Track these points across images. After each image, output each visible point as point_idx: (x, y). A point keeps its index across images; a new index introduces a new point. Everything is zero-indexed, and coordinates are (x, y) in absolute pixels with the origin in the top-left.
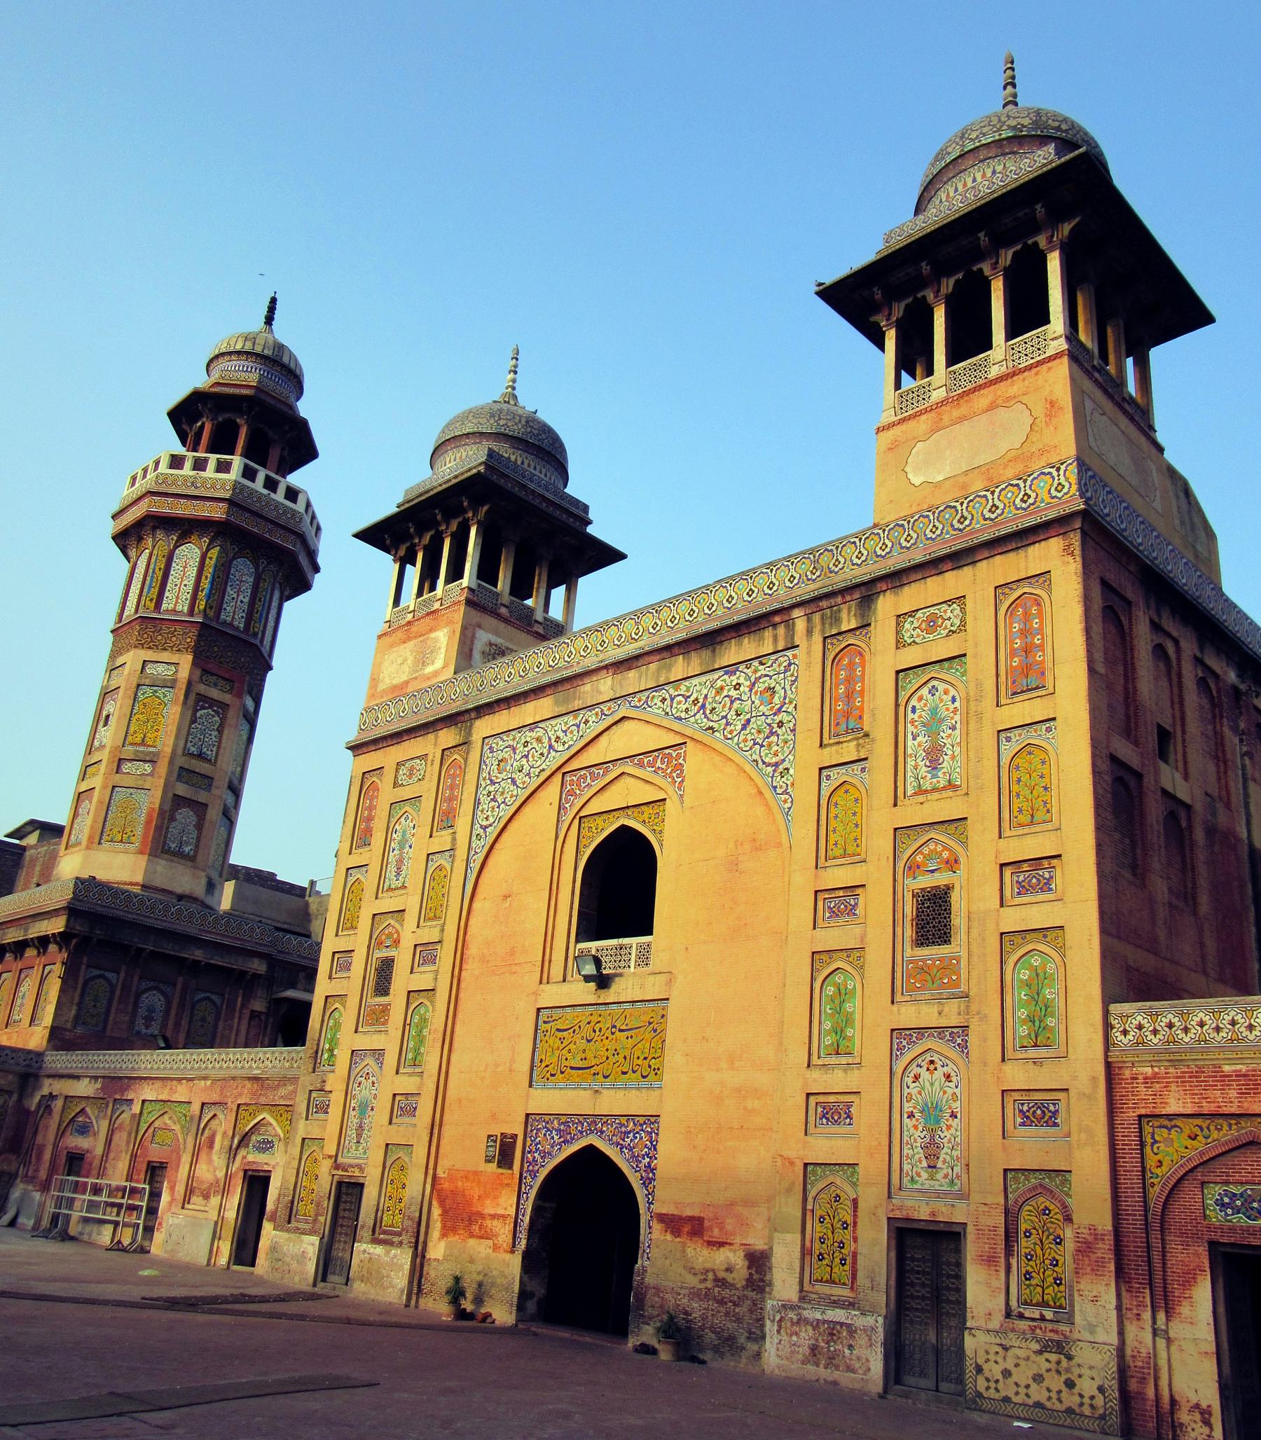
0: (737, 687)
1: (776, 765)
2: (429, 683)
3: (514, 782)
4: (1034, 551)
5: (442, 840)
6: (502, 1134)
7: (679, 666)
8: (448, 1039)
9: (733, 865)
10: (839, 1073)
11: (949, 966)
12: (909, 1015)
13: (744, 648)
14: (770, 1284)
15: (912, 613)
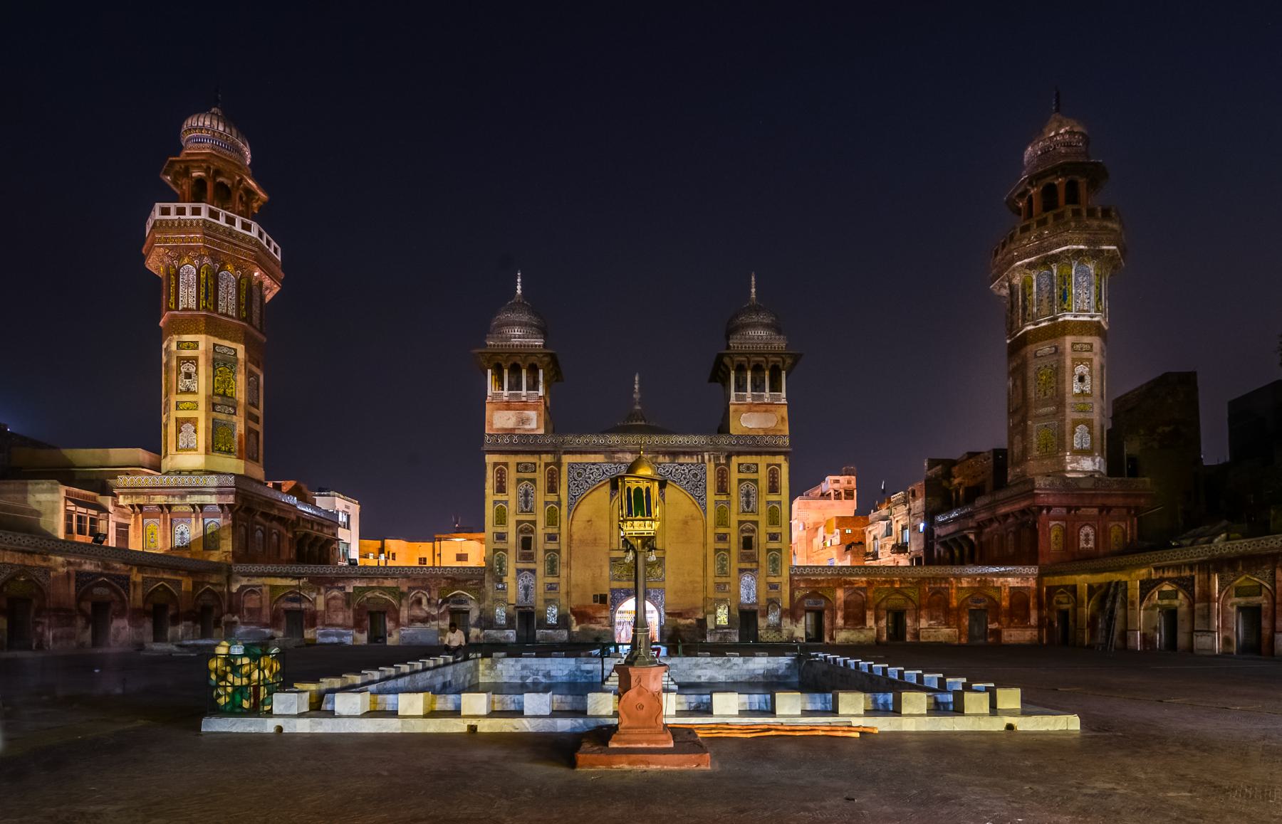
0: (684, 470)
1: (700, 497)
2: (529, 433)
3: (587, 482)
4: (777, 457)
5: (552, 497)
6: (601, 595)
7: (661, 459)
8: (569, 565)
9: (686, 523)
10: (724, 578)
11: (753, 555)
12: (743, 566)
13: (687, 460)
14: (707, 626)
15: (743, 464)
